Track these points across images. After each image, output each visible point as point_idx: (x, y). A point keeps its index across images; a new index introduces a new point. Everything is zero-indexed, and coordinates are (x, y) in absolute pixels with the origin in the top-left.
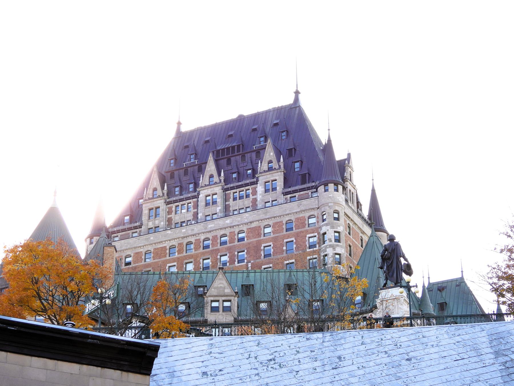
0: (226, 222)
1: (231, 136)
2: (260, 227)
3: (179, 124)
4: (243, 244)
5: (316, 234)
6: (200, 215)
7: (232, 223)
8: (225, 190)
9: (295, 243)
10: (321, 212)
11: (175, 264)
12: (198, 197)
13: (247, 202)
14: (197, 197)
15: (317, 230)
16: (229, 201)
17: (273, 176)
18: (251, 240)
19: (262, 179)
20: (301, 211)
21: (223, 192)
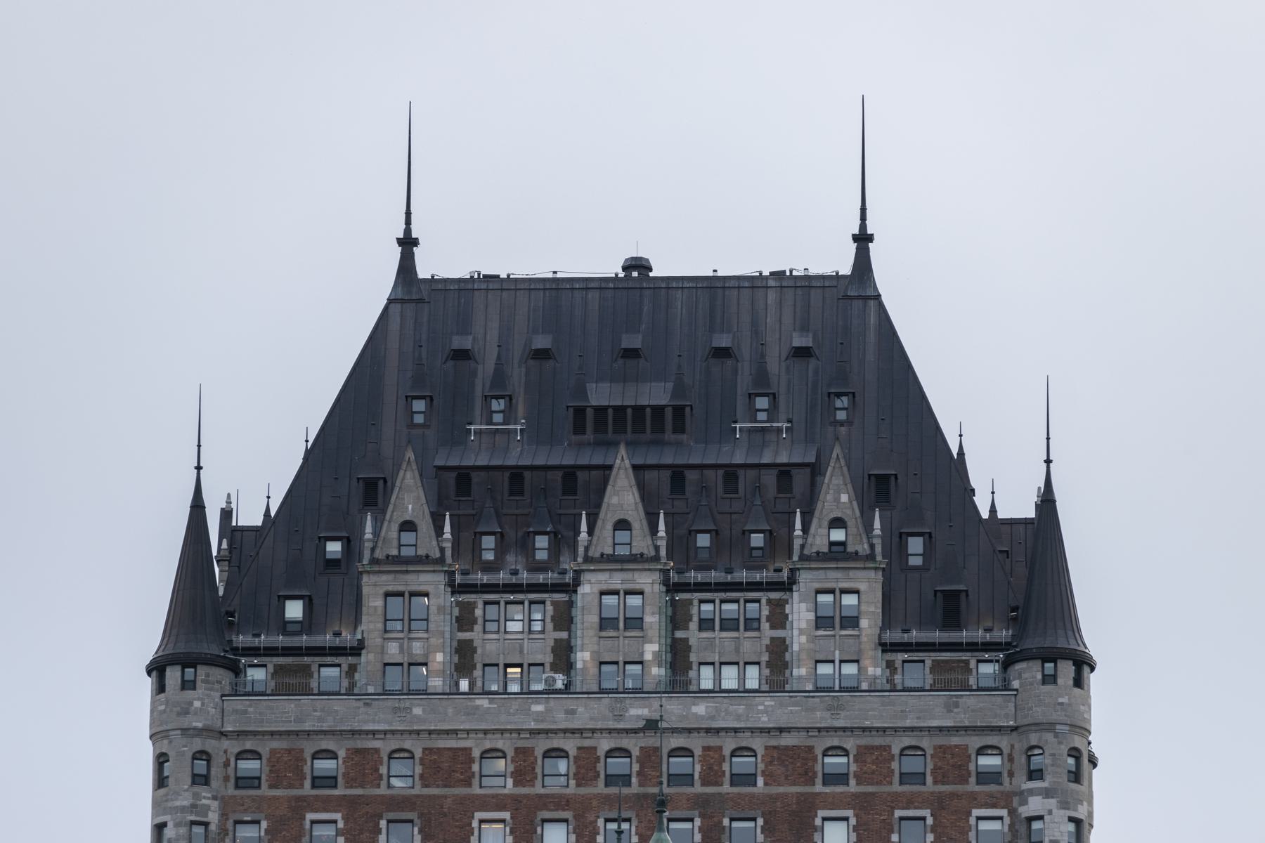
0: (695, 709)
1: (631, 354)
2: (810, 749)
3: (408, 243)
4: (752, 796)
5: (1004, 813)
6: (583, 658)
7: (712, 718)
8: (672, 588)
9: (934, 829)
10: (1026, 746)
11: (506, 815)
12: (576, 592)
13: (754, 644)
14: (570, 588)
15: (1008, 800)
16: (687, 628)
17: (851, 579)
18: (781, 790)
19: (808, 581)
20: (956, 730)
21: (667, 591)
